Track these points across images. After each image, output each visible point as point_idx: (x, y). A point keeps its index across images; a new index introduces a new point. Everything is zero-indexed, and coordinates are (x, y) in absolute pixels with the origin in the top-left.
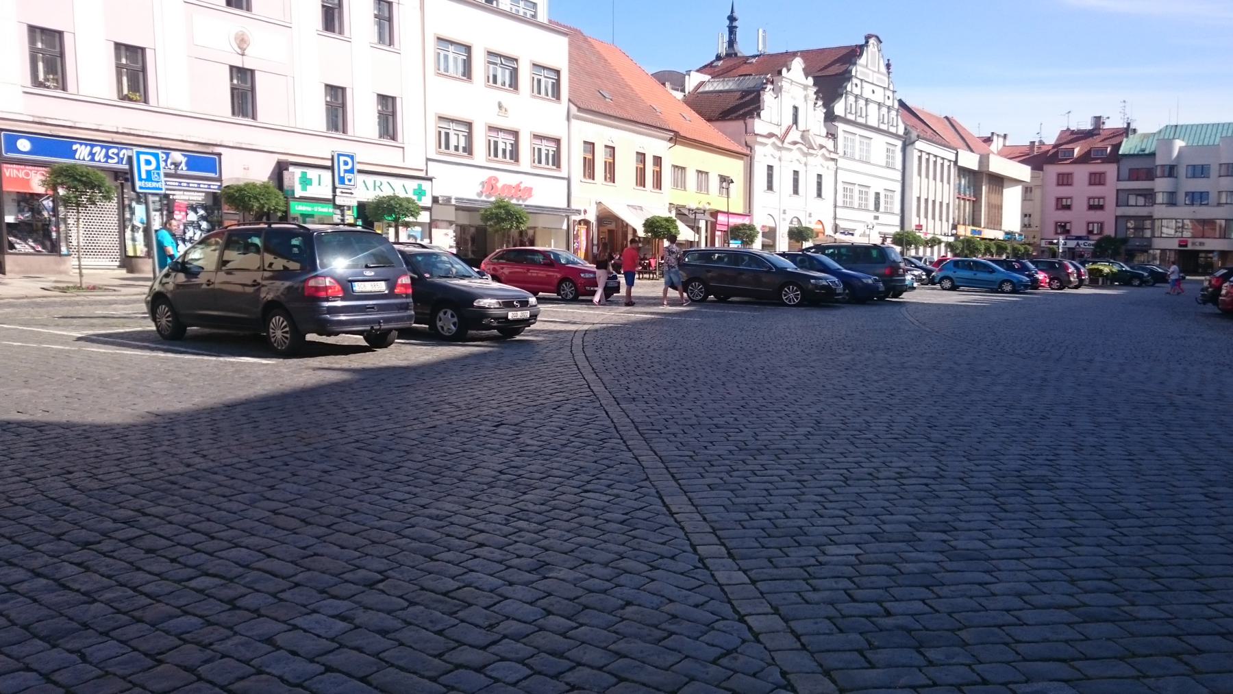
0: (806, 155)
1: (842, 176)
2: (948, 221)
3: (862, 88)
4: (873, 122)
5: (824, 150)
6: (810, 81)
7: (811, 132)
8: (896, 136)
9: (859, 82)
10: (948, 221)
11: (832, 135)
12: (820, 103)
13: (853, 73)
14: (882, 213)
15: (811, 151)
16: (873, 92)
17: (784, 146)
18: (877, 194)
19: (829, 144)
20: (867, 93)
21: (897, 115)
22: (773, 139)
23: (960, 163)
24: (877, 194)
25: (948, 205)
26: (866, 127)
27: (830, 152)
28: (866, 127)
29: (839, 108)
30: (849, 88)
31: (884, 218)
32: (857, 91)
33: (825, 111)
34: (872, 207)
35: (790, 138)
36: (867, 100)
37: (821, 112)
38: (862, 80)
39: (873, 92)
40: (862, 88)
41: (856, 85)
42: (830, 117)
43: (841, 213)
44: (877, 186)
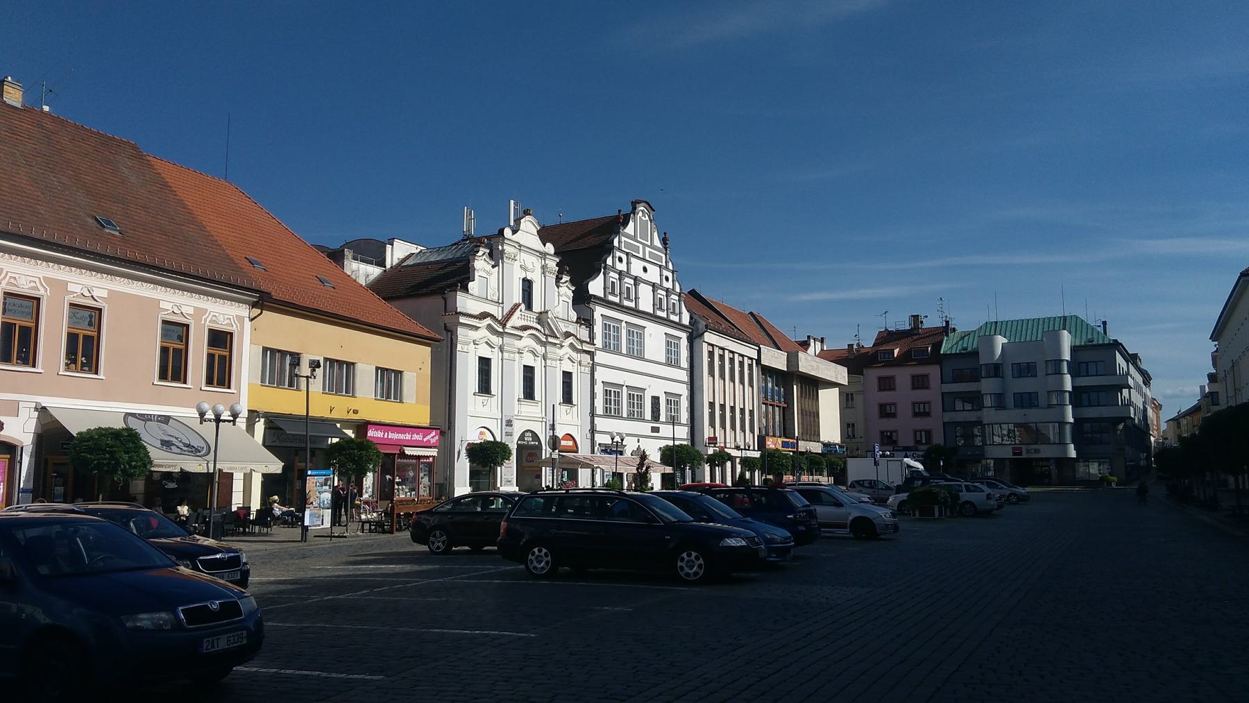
0: (544, 344)
1: (601, 375)
2: (752, 430)
3: (628, 263)
4: (646, 305)
5: (571, 340)
6: (550, 248)
7: (550, 315)
8: (679, 326)
9: (624, 257)
10: (752, 430)
11: (586, 321)
12: (566, 278)
13: (616, 243)
14: (662, 423)
15: (550, 340)
16: (645, 270)
17: (506, 331)
18: (655, 400)
19: (583, 333)
20: (637, 268)
21: (679, 301)
22: (488, 321)
23: (764, 362)
24: (655, 400)
25: (752, 412)
26: (636, 312)
27: (582, 342)
28: (636, 312)
29: (596, 287)
30: (609, 261)
31: (666, 430)
32: (622, 267)
33: (573, 288)
34: (648, 416)
35: (516, 320)
36: (635, 279)
37: (567, 291)
38: (627, 254)
39: (645, 270)
40: (628, 263)
41: (620, 260)
42: (582, 299)
43: (601, 423)
44: (655, 388)
